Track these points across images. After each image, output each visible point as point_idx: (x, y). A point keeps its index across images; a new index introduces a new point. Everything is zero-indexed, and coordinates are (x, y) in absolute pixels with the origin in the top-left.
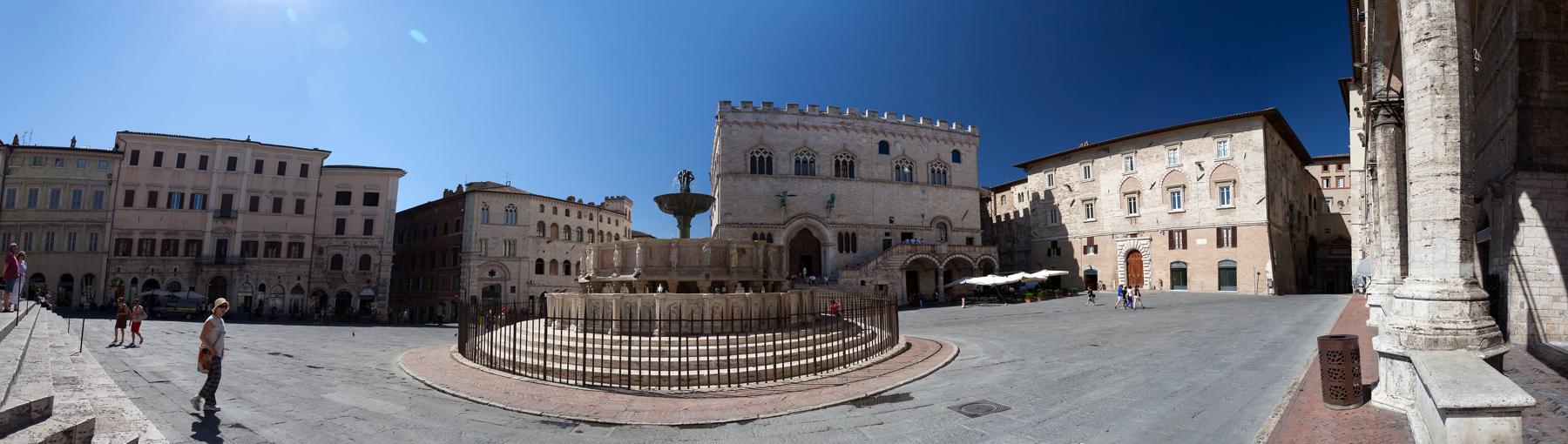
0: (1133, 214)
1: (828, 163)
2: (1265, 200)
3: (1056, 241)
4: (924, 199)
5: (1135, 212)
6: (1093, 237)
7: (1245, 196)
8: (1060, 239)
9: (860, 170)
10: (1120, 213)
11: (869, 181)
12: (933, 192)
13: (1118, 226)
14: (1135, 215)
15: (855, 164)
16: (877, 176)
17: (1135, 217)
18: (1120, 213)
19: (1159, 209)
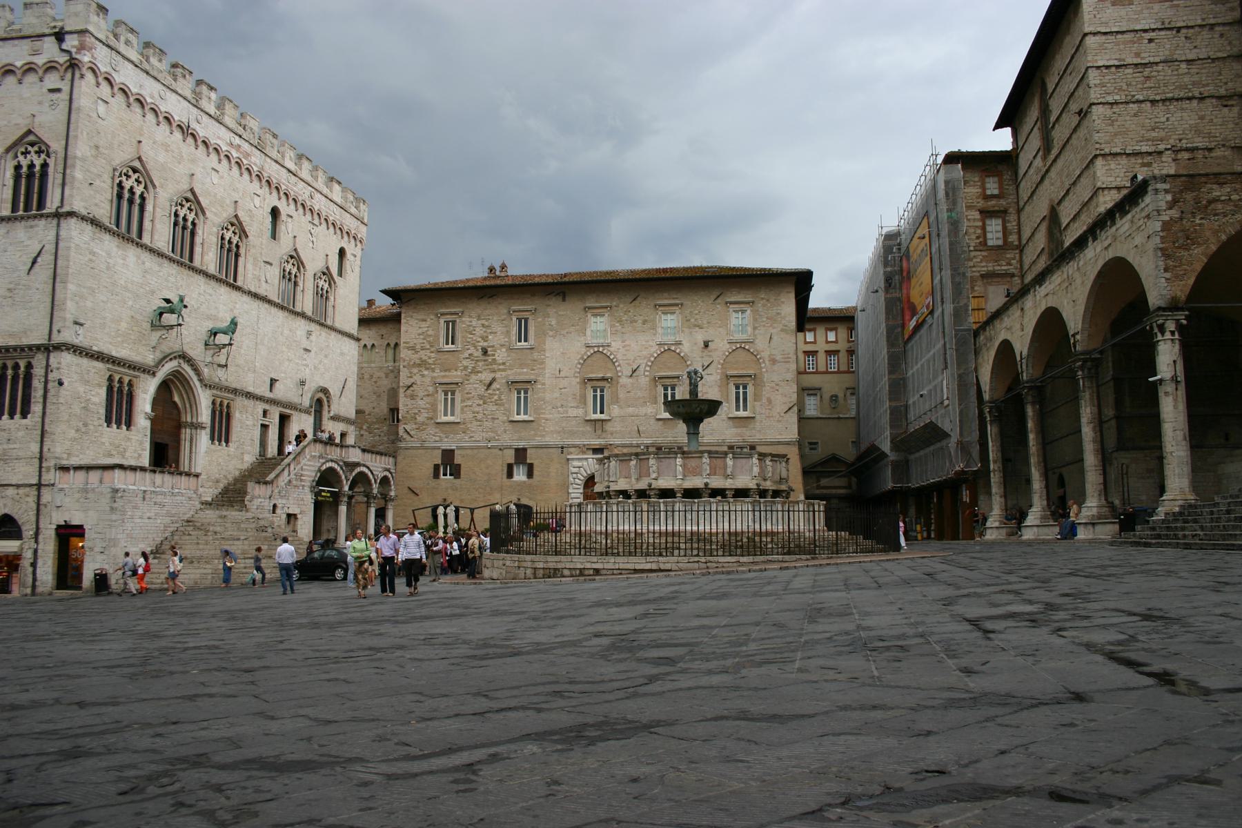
0: (598, 416)
1: (215, 240)
2: (795, 408)
3: (453, 451)
4: (307, 350)
5: (602, 412)
6: (525, 450)
7: (769, 401)
8: (459, 448)
9: (249, 273)
10: (580, 412)
11: (255, 296)
12: (319, 335)
13: (572, 434)
14: (603, 417)
15: (242, 251)
16: (262, 292)
17: (603, 421)
18: (580, 412)
19: (643, 411)
